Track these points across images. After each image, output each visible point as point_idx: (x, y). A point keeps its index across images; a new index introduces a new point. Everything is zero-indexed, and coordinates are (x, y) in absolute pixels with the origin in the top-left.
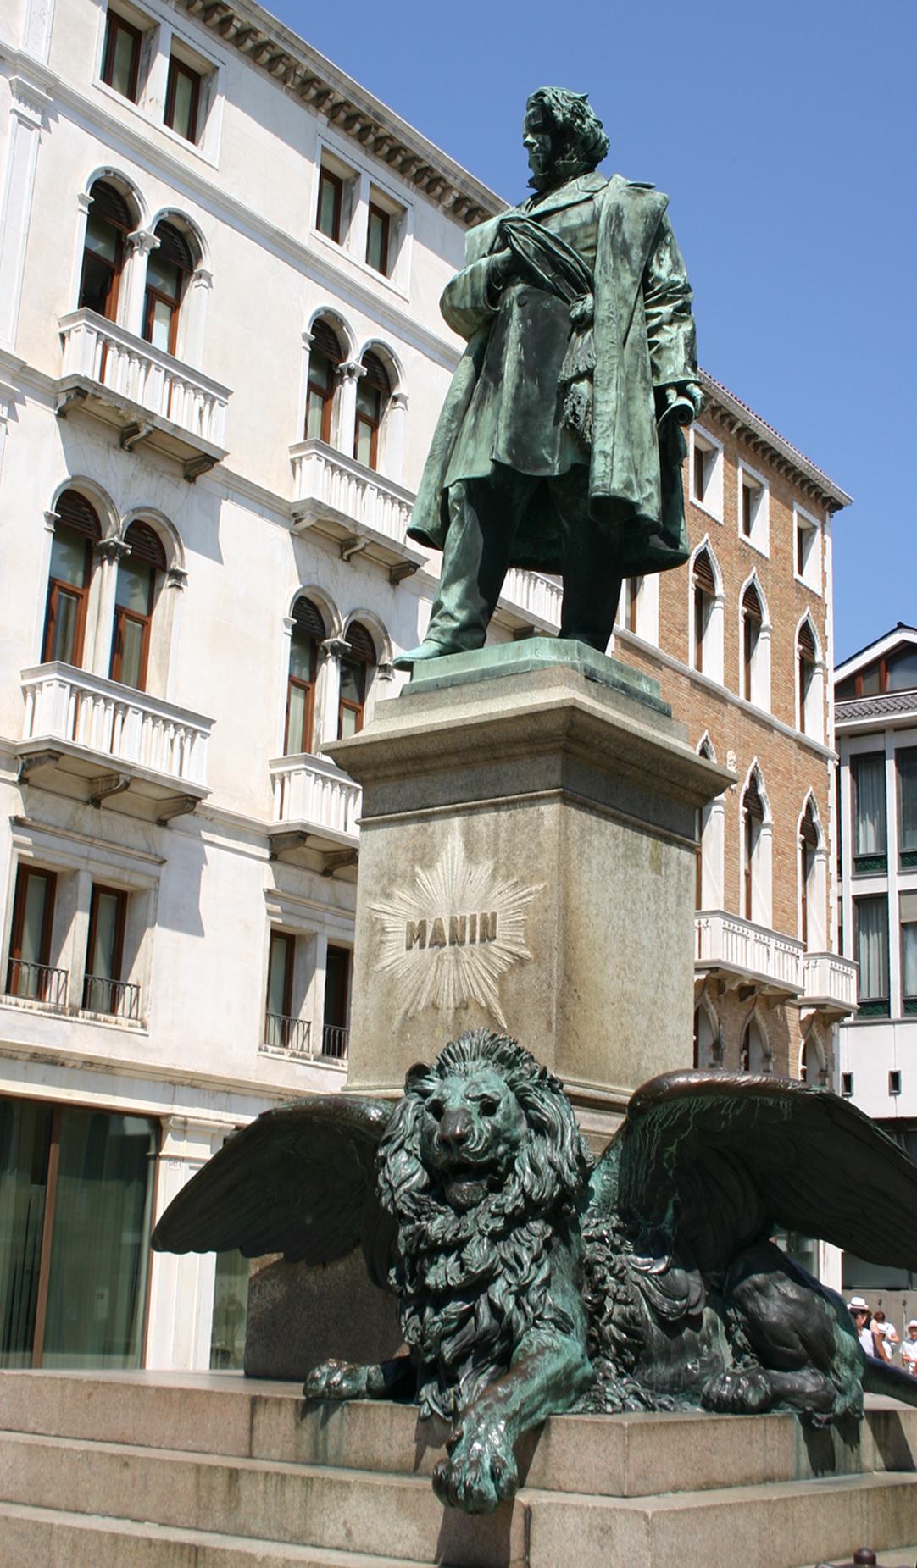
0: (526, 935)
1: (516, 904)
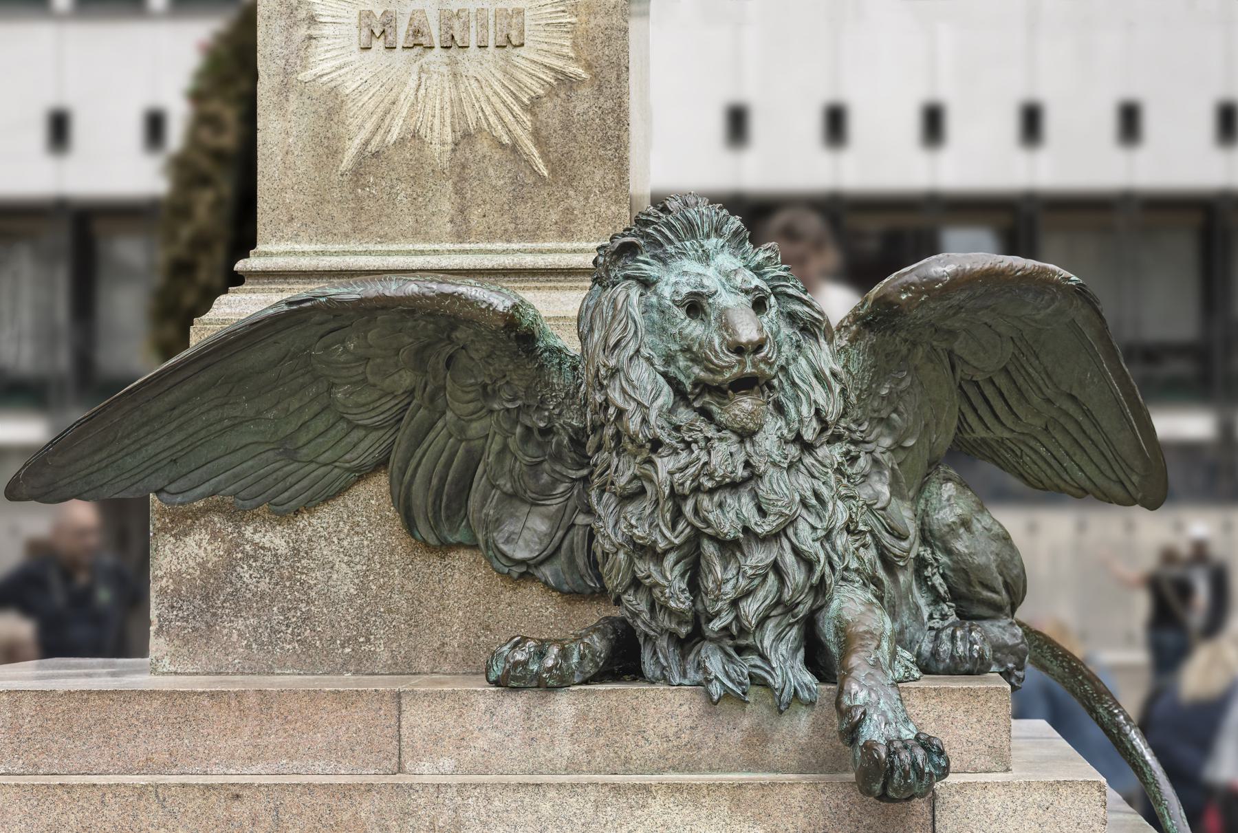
0: (575, 45)
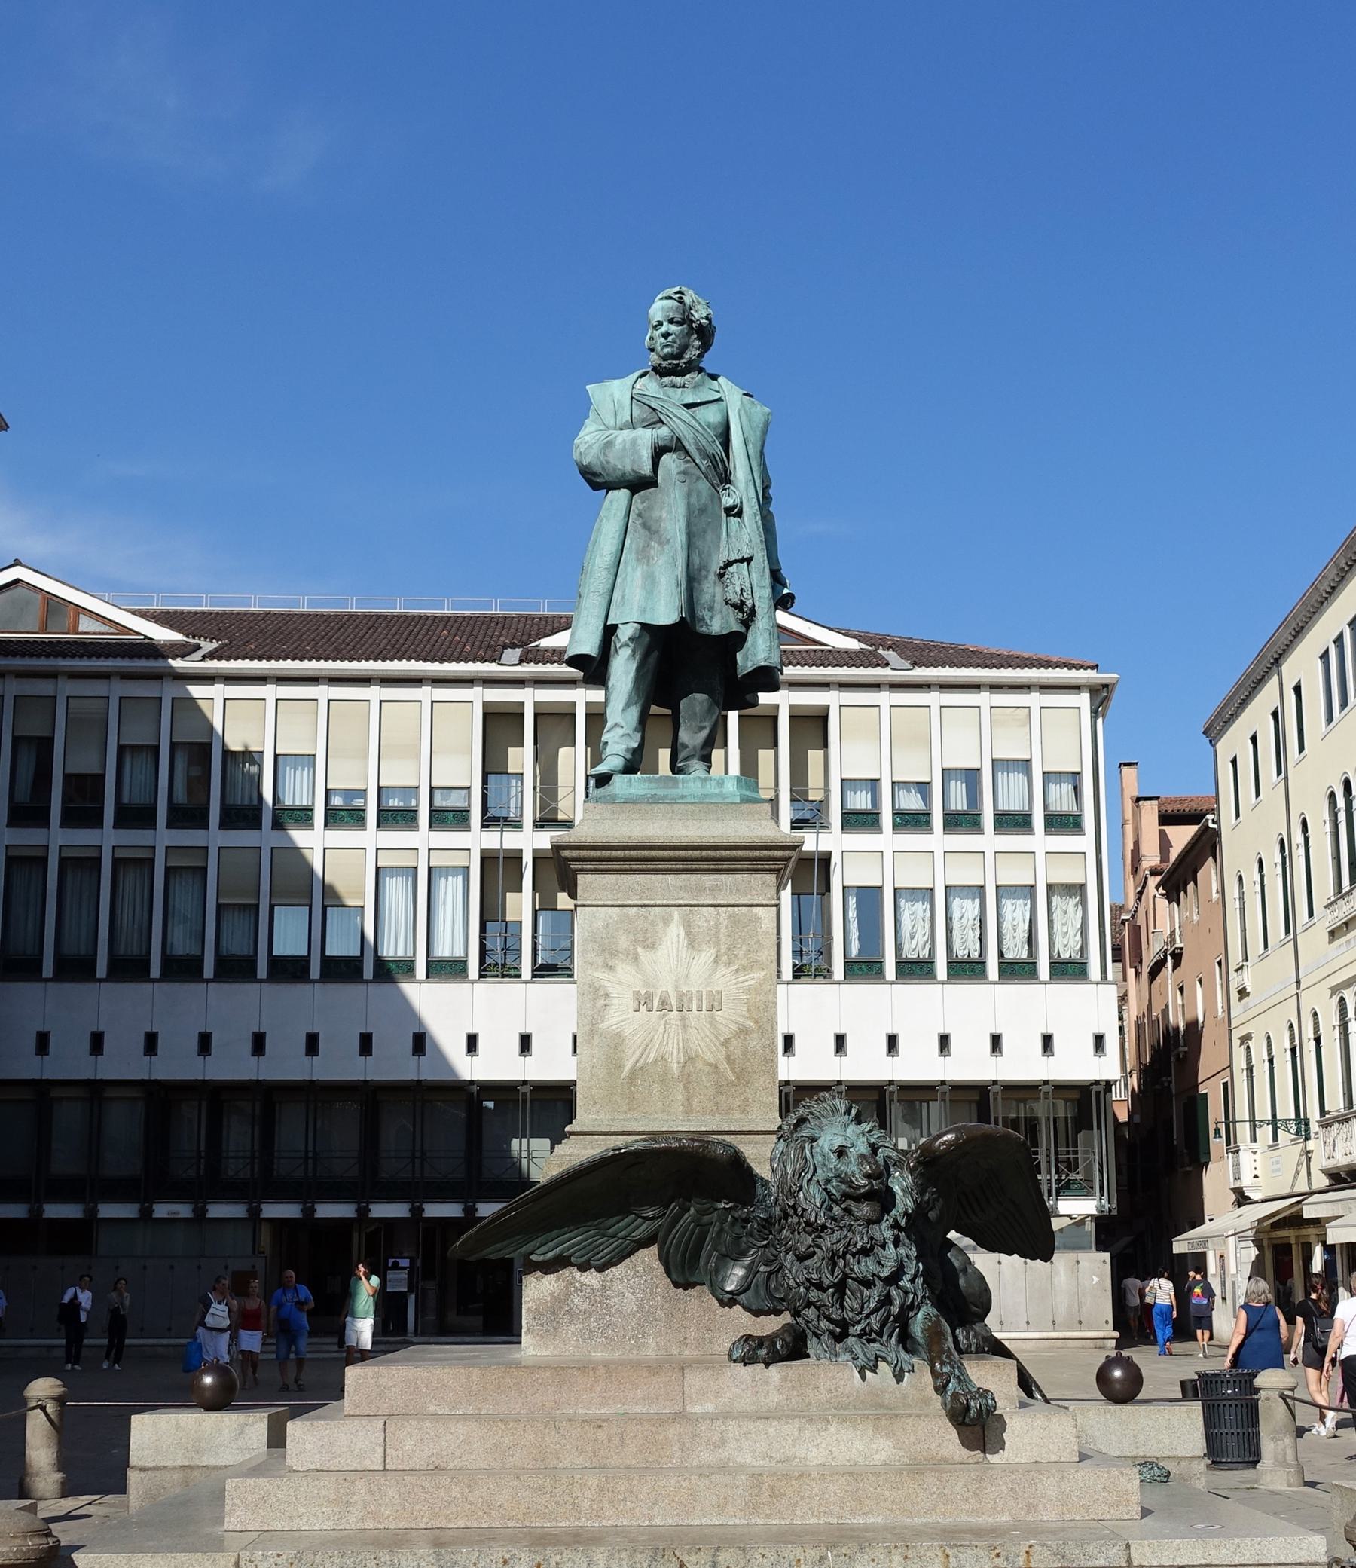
0: (749, 1011)
1: (739, 985)
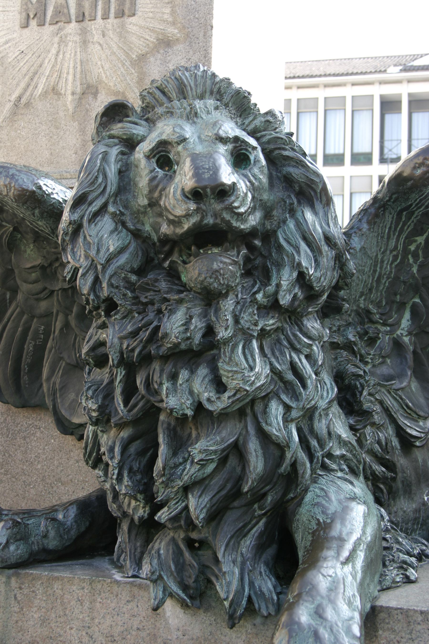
0: (173, 12)
